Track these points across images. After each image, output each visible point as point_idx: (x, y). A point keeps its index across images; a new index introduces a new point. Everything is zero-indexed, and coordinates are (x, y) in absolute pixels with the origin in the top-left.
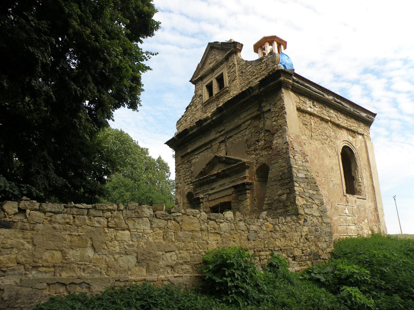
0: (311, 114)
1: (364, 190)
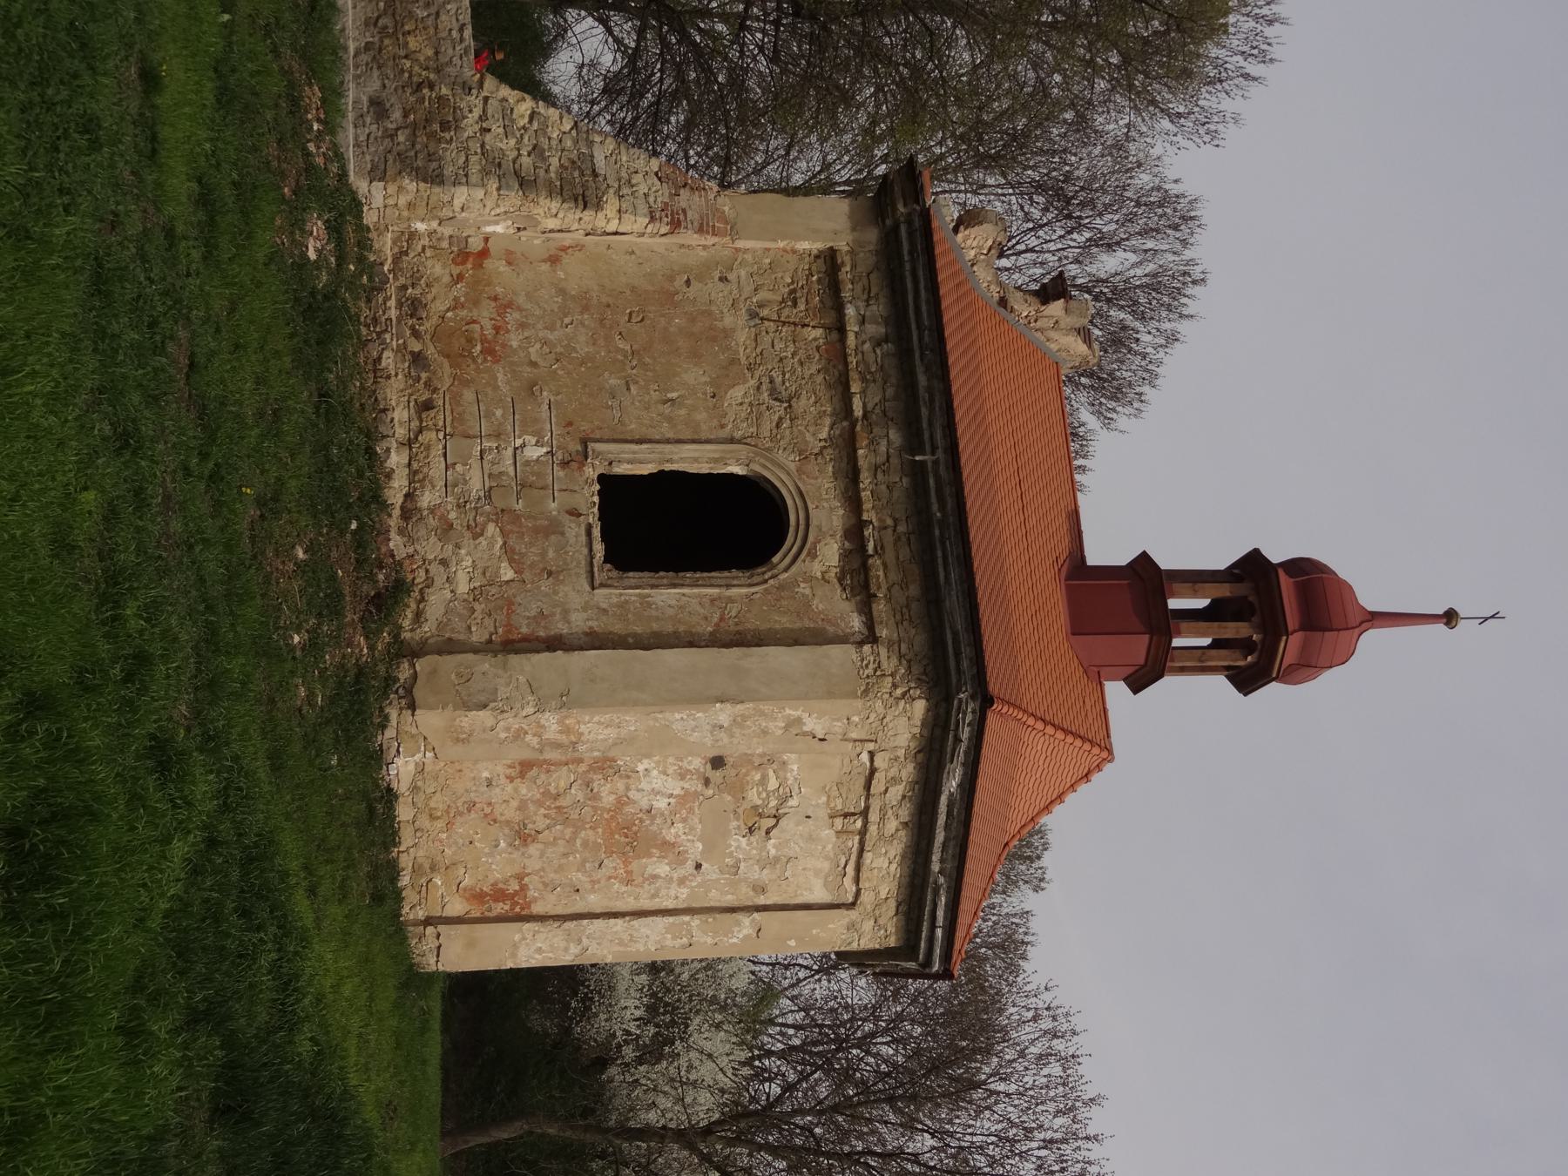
0: (841, 330)
1: (626, 582)
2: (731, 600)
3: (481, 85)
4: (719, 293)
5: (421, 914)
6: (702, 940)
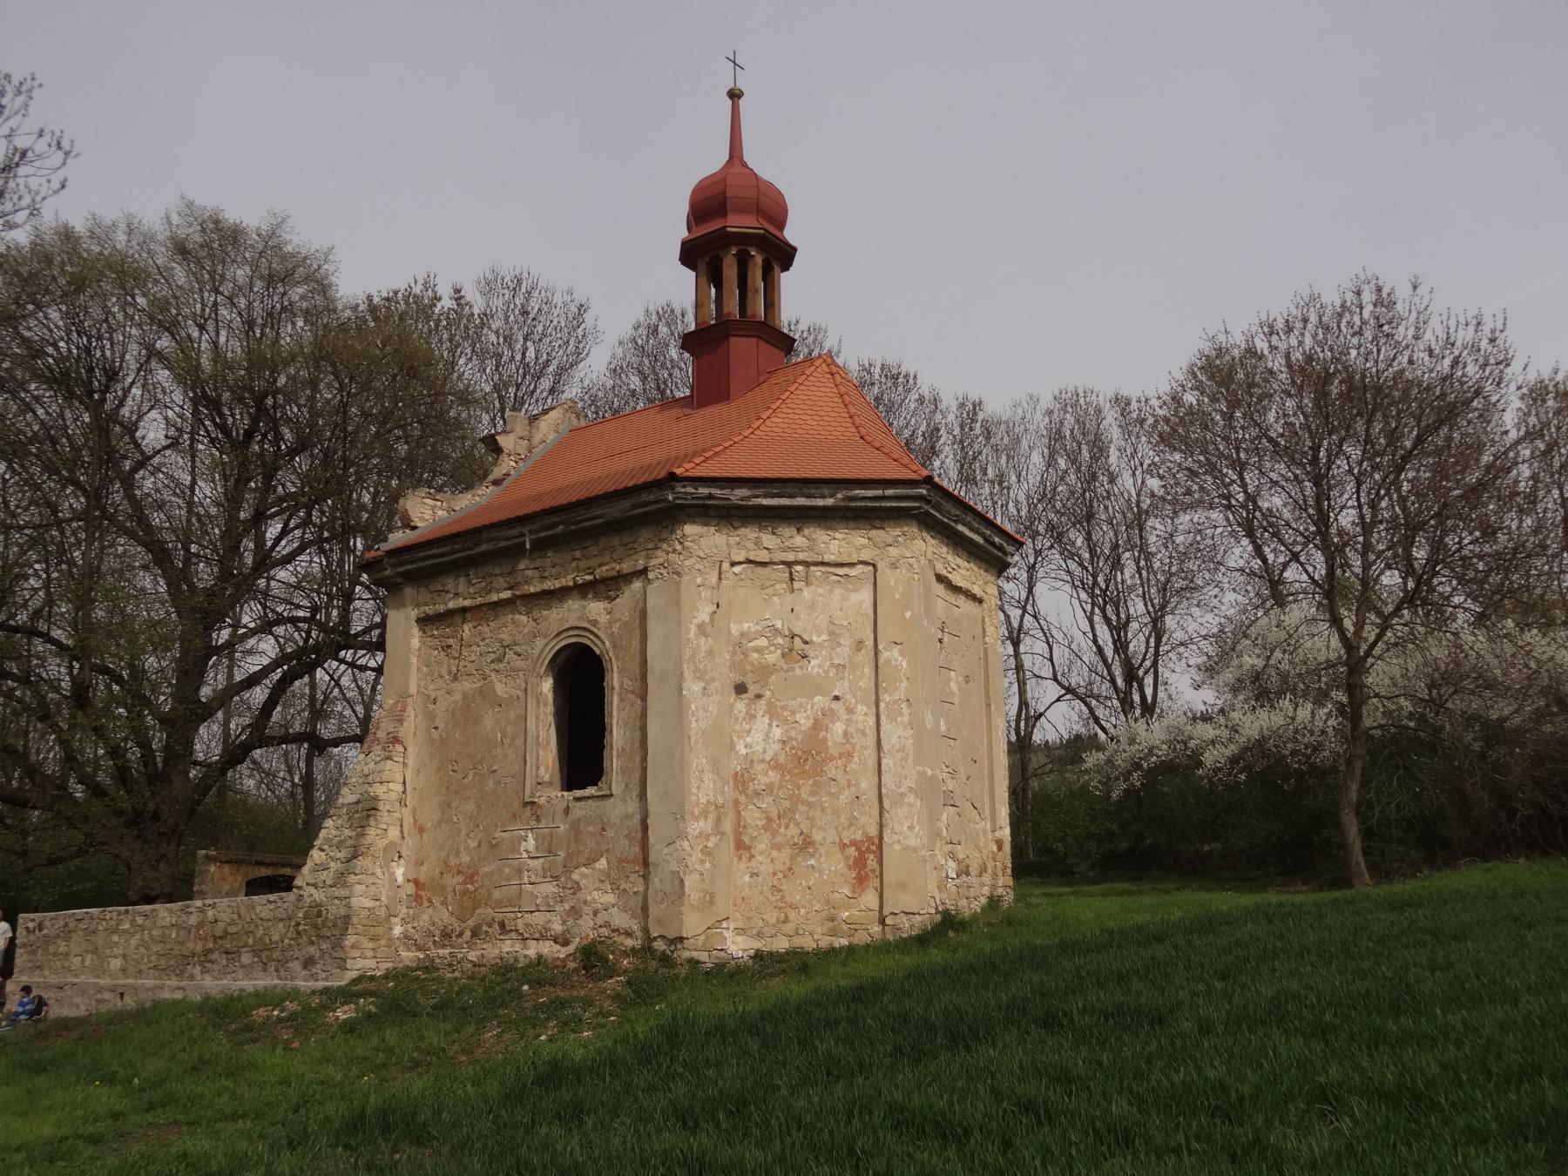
0: (464, 610)
2: (621, 686)
3: (300, 888)
4: (442, 706)
5: (877, 928)
6: (903, 690)
